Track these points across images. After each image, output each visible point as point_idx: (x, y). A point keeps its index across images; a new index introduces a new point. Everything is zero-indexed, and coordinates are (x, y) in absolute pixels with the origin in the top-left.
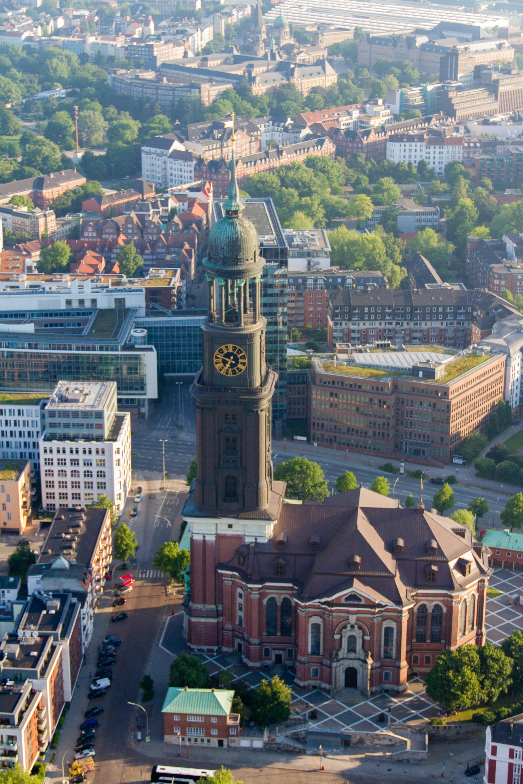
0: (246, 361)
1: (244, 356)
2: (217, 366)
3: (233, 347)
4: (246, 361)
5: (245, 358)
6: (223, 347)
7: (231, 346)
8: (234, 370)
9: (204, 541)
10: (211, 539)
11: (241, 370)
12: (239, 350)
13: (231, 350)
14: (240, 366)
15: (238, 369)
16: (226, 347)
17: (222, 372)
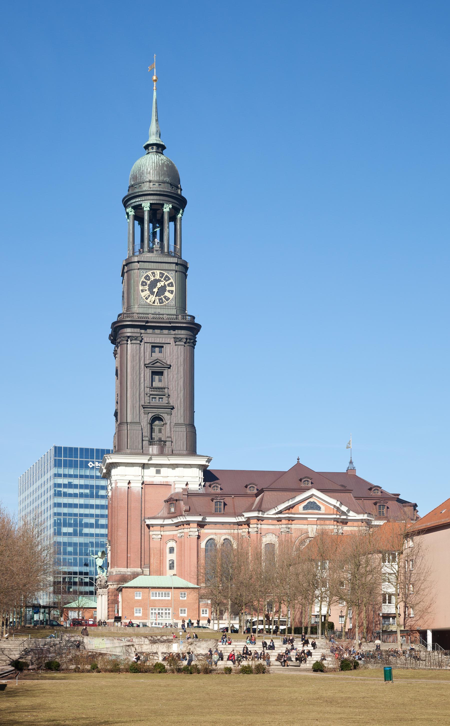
0: (173, 289)
1: (171, 283)
3: (160, 273)
4: (173, 289)
5: (172, 286)
6: (149, 273)
7: (158, 272)
8: (161, 299)
10: (136, 486)
11: (169, 299)
12: (166, 276)
14: (167, 294)
15: (165, 297)
16: (153, 273)
17: (148, 301)
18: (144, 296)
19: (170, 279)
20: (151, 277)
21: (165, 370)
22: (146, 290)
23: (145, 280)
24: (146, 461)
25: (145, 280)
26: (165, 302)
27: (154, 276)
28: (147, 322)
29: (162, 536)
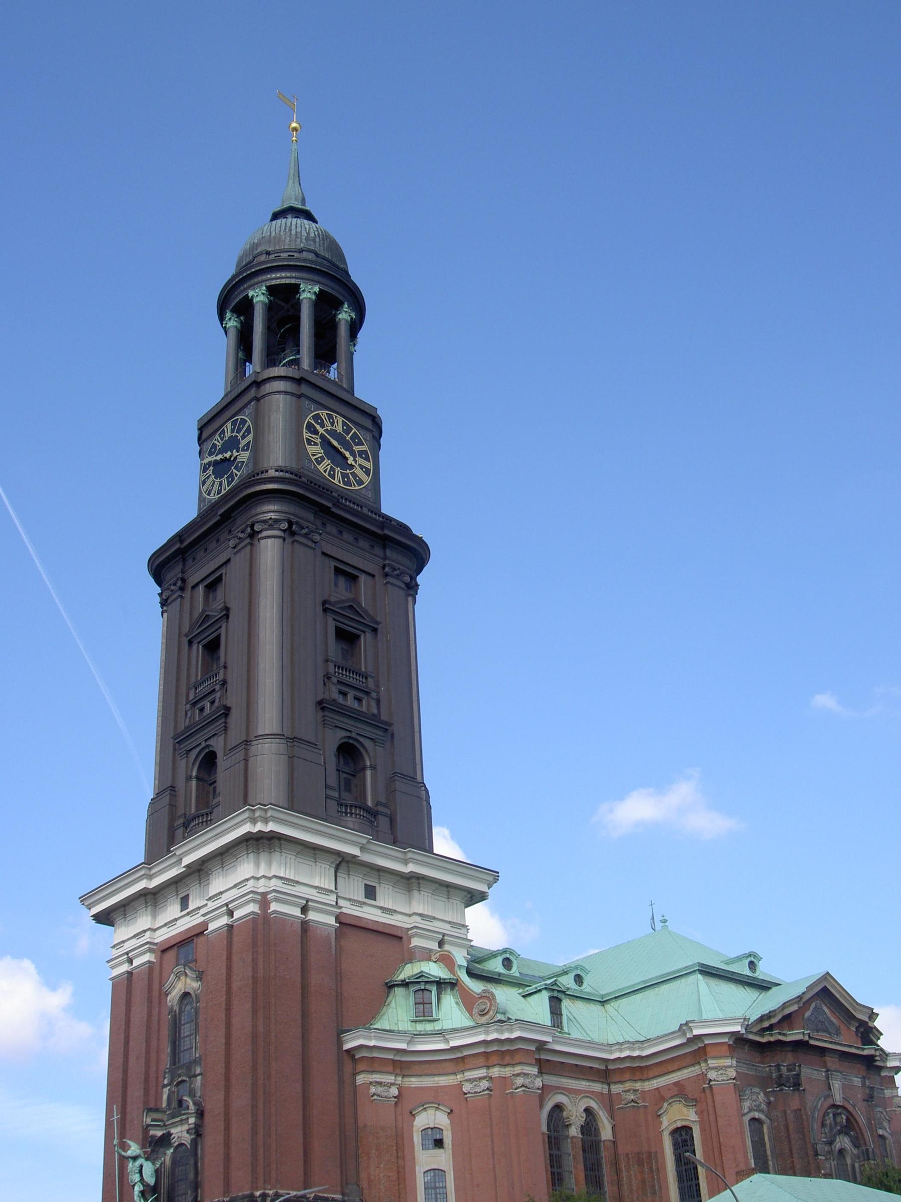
0: (369, 465)
2: (311, 449)
3: (344, 424)
4: (369, 465)
6: (323, 413)
9: (305, 926)
11: (360, 482)
13: (339, 429)
15: (355, 475)
17: (321, 468)
18: (313, 455)
19: (364, 445)
20: (325, 421)
21: (364, 632)
22: (316, 444)
23: (313, 422)
24: (355, 851)
25: (313, 422)
26: (355, 486)
27: (332, 424)
28: (337, 504)
29: (400, 1089)
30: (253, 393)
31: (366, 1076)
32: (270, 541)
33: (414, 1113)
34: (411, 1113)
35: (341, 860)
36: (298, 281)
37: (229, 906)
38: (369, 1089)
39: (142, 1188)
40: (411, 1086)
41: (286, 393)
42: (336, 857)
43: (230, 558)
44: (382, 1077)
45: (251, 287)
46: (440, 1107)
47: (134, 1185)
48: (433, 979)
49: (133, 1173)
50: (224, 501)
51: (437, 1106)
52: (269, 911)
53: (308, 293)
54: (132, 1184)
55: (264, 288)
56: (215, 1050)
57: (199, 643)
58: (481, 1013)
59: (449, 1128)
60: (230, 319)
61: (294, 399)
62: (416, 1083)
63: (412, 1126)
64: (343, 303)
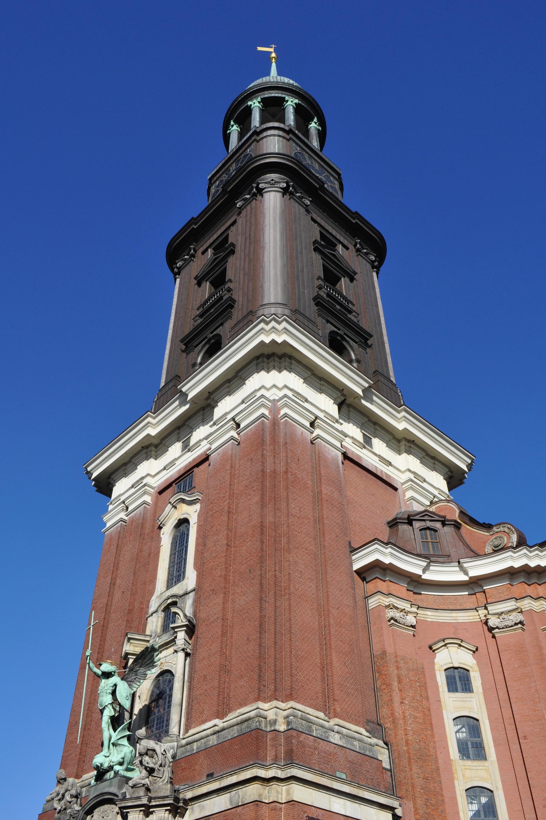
30: (253, 138)
31: (381, 597)
32: (272, 194)
33: (434, 648)
34: (430, 648)
35: (343, 398)
36: (283, 96)
37: (236, 420)
38: (385, 613)
39: (113, 713)
40: (427, 619)
41: (279, 136)
42: (340, 394)
43: (236, 219)
44: (398, 602)
45: (251, 100)
46: (462, 644)
47: (104, 708)
48: (437, 518)
49: (105, 694)
50: (233, 180)
51: (459, 642)
52: (279, 416)
53: (291, 102)
54: (101, 708)
55: (260, 98)
56: (214, 554)
57: (206, 281)
58: (494, 549)
59: (476, 668)
60: (232, 126)
61: (285, 140)
62: (433, 617)
63: (433, 663)
64: (314, 118)
